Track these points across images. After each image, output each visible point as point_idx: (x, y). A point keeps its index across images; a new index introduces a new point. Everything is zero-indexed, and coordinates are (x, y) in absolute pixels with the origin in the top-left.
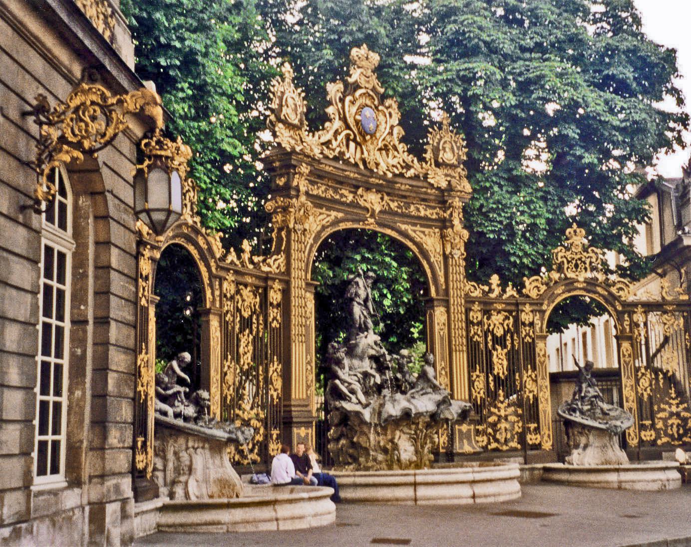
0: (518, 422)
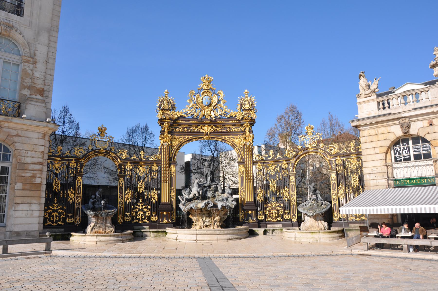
0: (281, 210)
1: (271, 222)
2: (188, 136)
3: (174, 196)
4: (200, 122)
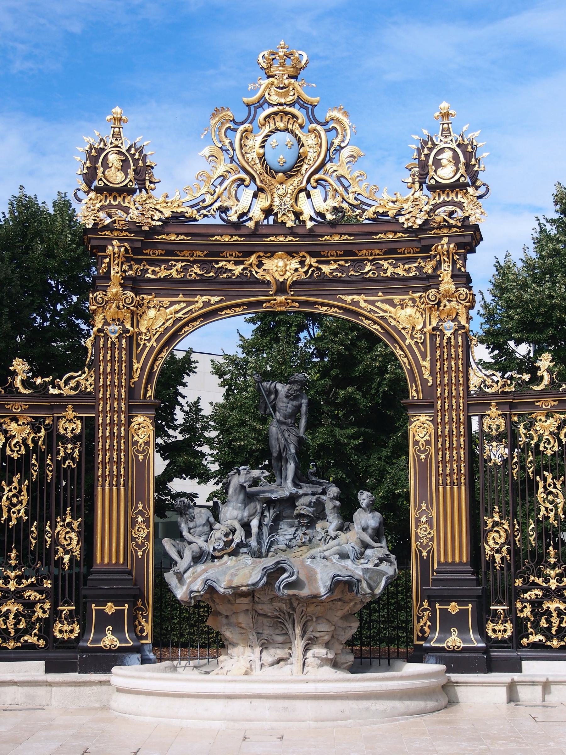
1: (540, 650)
2: (205, 298)
3: (147, 538)
4: (253, 240)
